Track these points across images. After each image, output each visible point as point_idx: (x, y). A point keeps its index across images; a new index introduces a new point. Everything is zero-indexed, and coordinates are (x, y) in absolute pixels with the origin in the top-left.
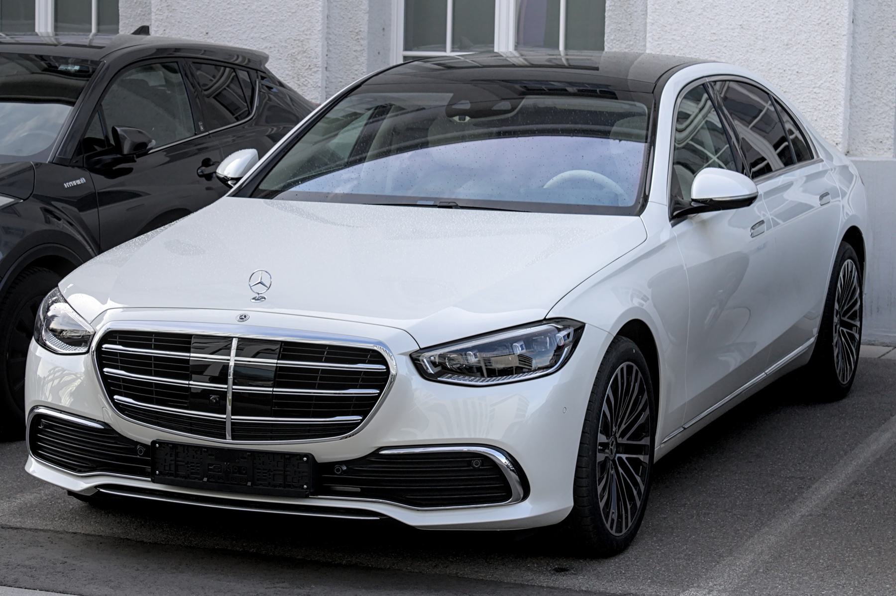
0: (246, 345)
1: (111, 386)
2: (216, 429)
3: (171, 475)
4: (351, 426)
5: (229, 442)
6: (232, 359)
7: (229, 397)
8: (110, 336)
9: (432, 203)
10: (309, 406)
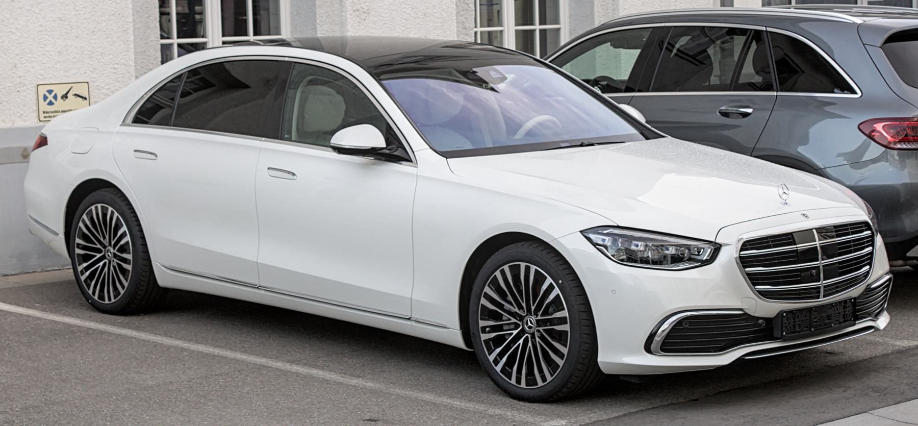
0: (823, 231)
1: (754, 279)
2: (815, 293)
3: (792, 333)
4: (868, 272)
5: (823, 300)
6: (817, 243)
7: (821, 268)
8: (747, 245)
9: (568, 145)
10: (851, 265)
